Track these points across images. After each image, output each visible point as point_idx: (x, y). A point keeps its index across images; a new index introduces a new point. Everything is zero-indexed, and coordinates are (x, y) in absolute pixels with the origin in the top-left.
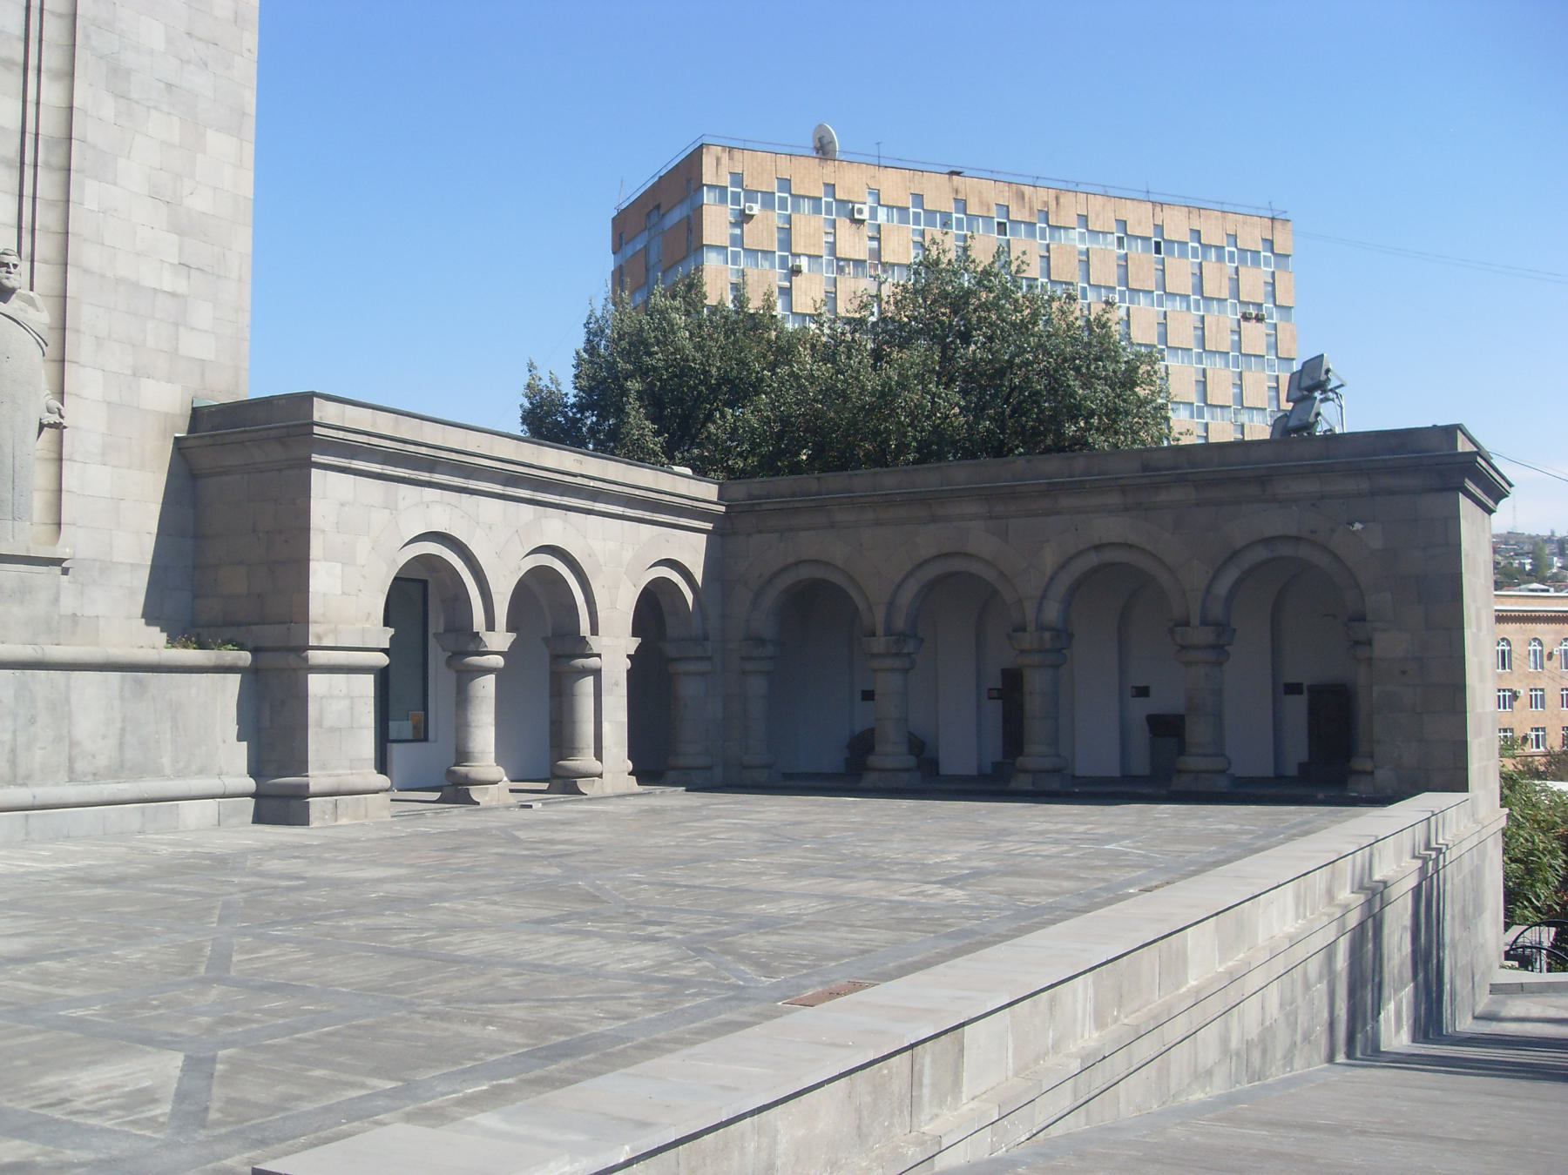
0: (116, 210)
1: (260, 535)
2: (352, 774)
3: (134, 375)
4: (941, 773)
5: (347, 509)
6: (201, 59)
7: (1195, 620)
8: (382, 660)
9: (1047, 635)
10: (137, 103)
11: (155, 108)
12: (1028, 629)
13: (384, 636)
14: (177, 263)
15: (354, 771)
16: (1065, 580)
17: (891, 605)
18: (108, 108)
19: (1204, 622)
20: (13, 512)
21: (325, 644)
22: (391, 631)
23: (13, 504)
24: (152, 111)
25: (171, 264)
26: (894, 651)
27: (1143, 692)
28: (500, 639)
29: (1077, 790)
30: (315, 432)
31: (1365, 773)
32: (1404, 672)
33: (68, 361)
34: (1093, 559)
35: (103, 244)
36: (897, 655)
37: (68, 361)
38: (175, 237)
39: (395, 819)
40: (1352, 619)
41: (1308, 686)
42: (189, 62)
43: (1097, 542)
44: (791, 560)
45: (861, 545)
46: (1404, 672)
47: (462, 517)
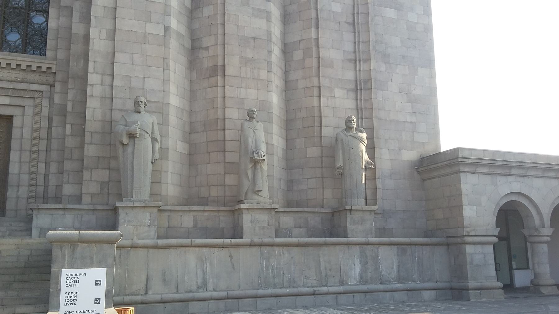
0: (388, 99)
1: (446, 198)
2: (487, 282)
3: (399, 150)
5: (476, 186)
6: (414, 46)
8: (496, 240)
10: (393, 64)
11: (399, 64)
13: (496, 232)
14: (411, 112)
15: (488, 281)
18: (383, 68)
20: (357, 197)
21: (470, 235)
22: (499, 229)
23: (357, 194)
24: (398, 66)
25: (409, 113)
28: (547, 231)
30: (459, 161)
33: (376, 148)
35: (385, 110)
37: (376, 148)
38: (410, 104)
39: (507, 299)
42: (410, 48)
47: (526, 186)
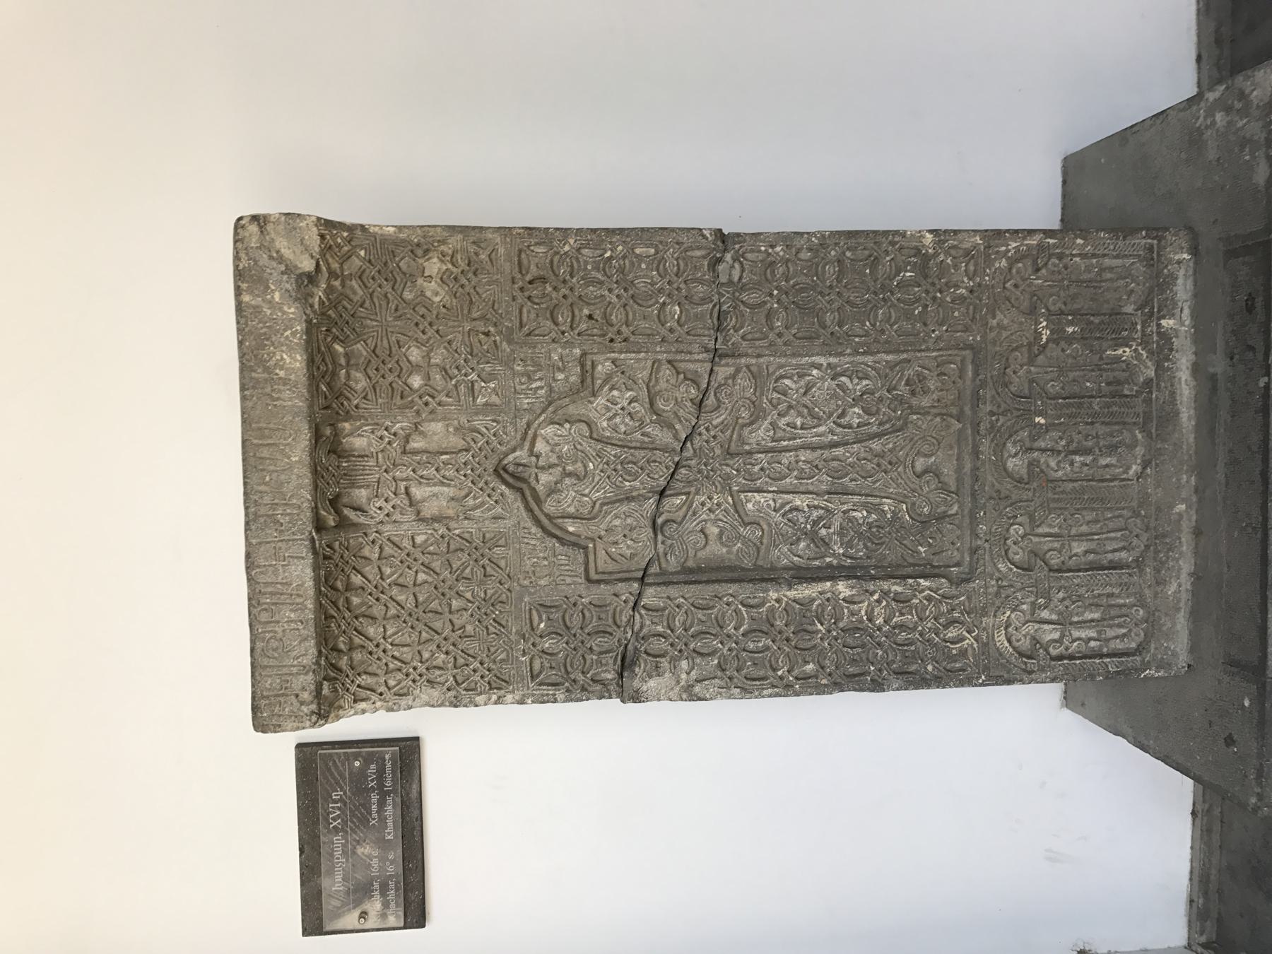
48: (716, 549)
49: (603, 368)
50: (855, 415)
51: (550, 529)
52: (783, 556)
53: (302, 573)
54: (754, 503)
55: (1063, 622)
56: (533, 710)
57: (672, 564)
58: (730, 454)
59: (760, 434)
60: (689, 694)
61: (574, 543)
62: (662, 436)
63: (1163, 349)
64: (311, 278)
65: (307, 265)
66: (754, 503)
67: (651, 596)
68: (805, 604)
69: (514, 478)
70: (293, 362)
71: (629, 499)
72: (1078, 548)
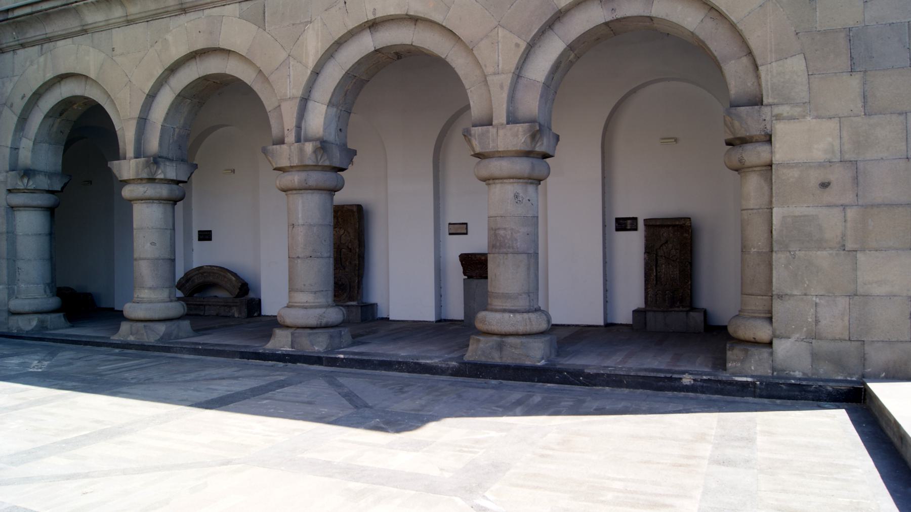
4: (263, 313)
7: (500, 116)
9: (309, 147)
12: (286, 140)
16: (333, 74)
17: (143, 121)
19: (512, 119)
26: (145, 176)
27: (461, 229)
29: (342, 356)
31: (756, 343)
32: (825, 185)
34: (367, 44)
36: (152, 180)
40: (735, 105)
41: (645, 220)
43: (371, 17)
44: (49, 76)
45: (113, 49)
46: (825, 185)
48: (659, 262)
49: (678, 251)
50: (672, 276)
51: (662, 246)
52: (658, 268)
53: (658, 223)
54: (664, 266)
55: (650, 297)
56: (644, 243)
57: (658, 258)
58: (669, 263)
59: (670, 266)
60: (645, 259)
61: (660, 248)
62: (671, 256)
63: (678, 307)
64: (684, 224)
65: (686, 224)
66: (664, 266)
67: (655, 255)
68: (653, 270)
69: (667, 242)
70: (677, 223)
71: (664, 253)
72: (658, 299)
